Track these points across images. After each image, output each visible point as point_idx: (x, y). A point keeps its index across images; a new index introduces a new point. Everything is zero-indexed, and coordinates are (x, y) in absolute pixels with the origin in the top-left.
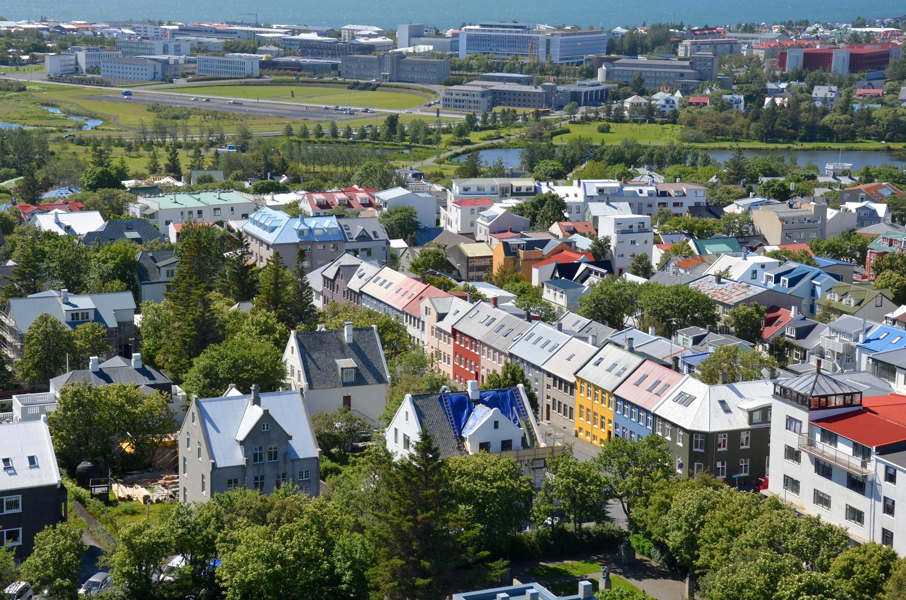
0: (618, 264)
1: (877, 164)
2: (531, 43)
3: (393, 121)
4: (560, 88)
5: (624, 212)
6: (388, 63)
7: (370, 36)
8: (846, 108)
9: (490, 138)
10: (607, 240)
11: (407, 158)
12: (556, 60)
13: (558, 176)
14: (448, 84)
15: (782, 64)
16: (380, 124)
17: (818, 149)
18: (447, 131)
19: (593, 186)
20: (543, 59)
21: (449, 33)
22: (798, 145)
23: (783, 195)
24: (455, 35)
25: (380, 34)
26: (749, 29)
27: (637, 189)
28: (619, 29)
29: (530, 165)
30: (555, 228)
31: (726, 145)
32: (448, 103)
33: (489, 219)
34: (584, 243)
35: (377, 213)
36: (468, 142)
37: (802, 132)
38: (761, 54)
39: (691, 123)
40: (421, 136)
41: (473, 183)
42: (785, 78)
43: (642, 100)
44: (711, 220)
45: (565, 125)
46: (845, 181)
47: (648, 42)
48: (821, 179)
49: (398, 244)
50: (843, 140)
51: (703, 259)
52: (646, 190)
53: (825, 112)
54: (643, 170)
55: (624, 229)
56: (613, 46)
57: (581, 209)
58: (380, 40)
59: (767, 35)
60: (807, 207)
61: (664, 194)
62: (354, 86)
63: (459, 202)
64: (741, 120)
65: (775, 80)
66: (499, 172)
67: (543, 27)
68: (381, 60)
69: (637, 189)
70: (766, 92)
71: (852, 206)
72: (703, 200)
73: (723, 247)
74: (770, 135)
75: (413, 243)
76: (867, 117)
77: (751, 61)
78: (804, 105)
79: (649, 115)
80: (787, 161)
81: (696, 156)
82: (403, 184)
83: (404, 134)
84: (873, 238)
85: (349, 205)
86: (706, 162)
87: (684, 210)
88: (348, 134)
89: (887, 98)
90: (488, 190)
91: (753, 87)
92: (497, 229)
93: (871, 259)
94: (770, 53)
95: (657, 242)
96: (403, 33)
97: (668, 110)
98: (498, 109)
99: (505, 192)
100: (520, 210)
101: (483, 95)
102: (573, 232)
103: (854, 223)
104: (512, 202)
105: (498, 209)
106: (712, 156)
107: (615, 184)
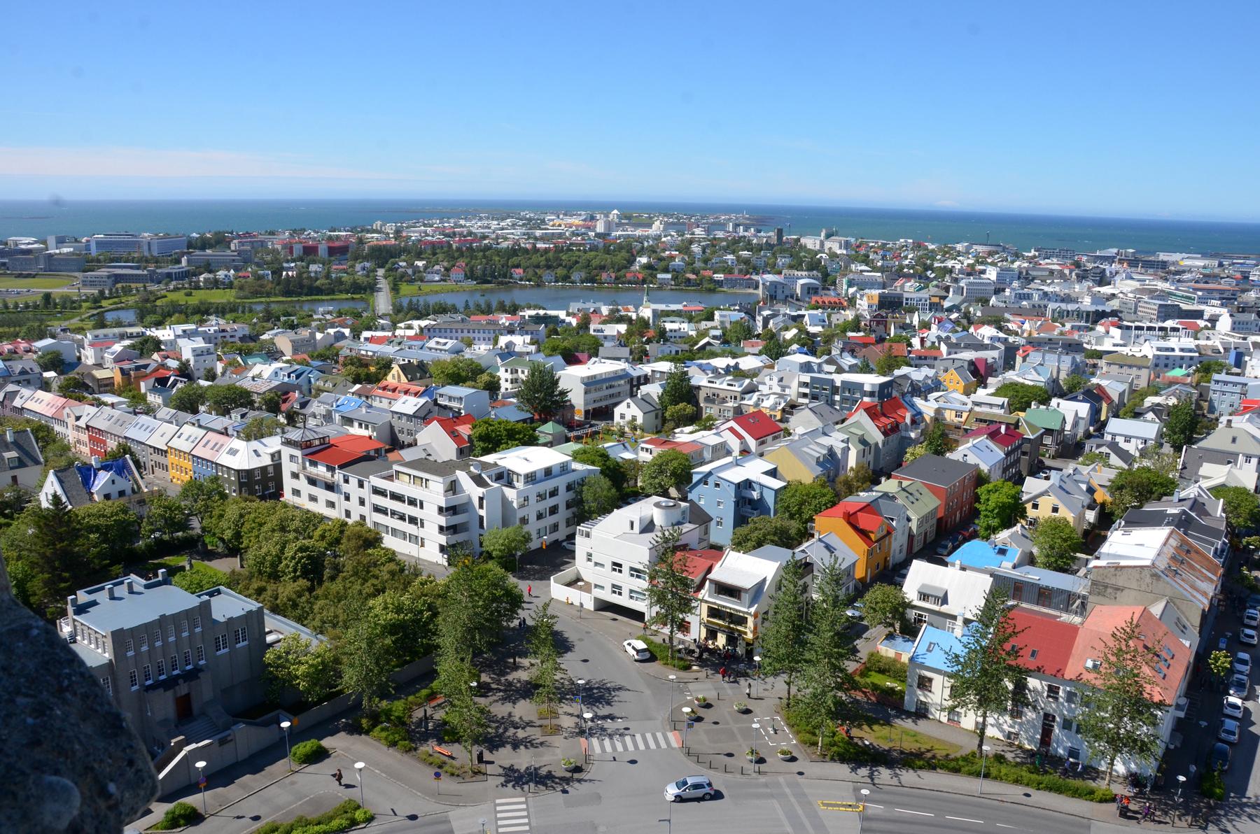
0: (197, 374)
1: (346, 307)
2: (138, 244)
3: (47, 297)
4: (159, 271)
5: (200, 343)
6: (42, 261)
7: (29, 244)
8: (328, 276)
9: (115, 303)
10: (188, 361)
11: (59, 319)
12: (155, 254)
13: (159, 324)
14: (85, 271)
15: (291, 252)
16: (39, 300)
17: (315, 300)
18: (85, 301)
19: (180, 328)
20: (146, 254)
21: (84, 240)
22: (305, 298)
23: (293, 327)
24: (88, 241)
25: (35, 242)
26: (272, 233)
27: (207, 329)
28: (194, 235)
29: (141, 319)
30: (156, 356)
31: (263, 300)
32: (85, 284)
33: (113, 354)
34: (173, 364)
35: (35, 357)
36: (101, 307)
37: (305, 291)
38: (279, 247)
39: (241, 288)
40: (68, 304)
41: (101, 332)
42: (293, 261)
43: (211, 276)
44: (252, 344)
45: (164, 292)
46: (328, 317)
47: (213, 242)
48: (315, 317)
49: (50, 374)
50: (328, 294)
51: (247, 368)
52: (212, 329)
53: (317, 279)
54: (211, 317)
55: (198, 353)
56: (191, 245)
57: (173, 343)
58: (36, 246)
59: (281, 237)
60: (304, 333)
61: (223, 331)
62: (20, 276)
63: (92, 345)
64: (270, 285)
65: (288, 261)
66: (119, 324)
67: (146, 235)
68: (37, 259)
69: (207, 329)
70: (283, 269)
71: (331, 331)
72: (247, 333)
73: (259, 359)
74: (287, 293)
75: (60, 373)
76: (339, 281)
77: (274, 251)
78: (305, 275)
79: (216, 284)
80: (298, 308)
81: (244, 307)
82: (53, 337)
83: (55, 305)
84: (342, 348)
85: (16, 352)
86: (251, 311)
87: (236, 339)
88: (16, 306)
89: (350, 270)
90: (111, 335)
91: (276, 266)
92: (118, 359)
93: (341, 359)
94: (285, 246)
95: (220, 359)
96: (51, 241)
97: (227, 281)
98: (119, 285)
99: (122, 337)
100: (133, 347)
101: (109, 277)
102: (168, 357)
103: (332, 340)
104: (127, 342)
105: (118, 347)
106: (254, 307)
107: (193, 327)
